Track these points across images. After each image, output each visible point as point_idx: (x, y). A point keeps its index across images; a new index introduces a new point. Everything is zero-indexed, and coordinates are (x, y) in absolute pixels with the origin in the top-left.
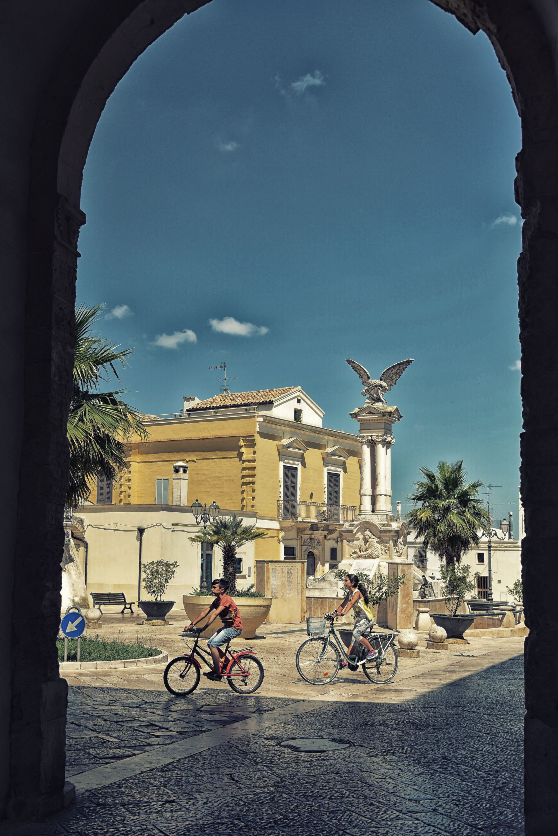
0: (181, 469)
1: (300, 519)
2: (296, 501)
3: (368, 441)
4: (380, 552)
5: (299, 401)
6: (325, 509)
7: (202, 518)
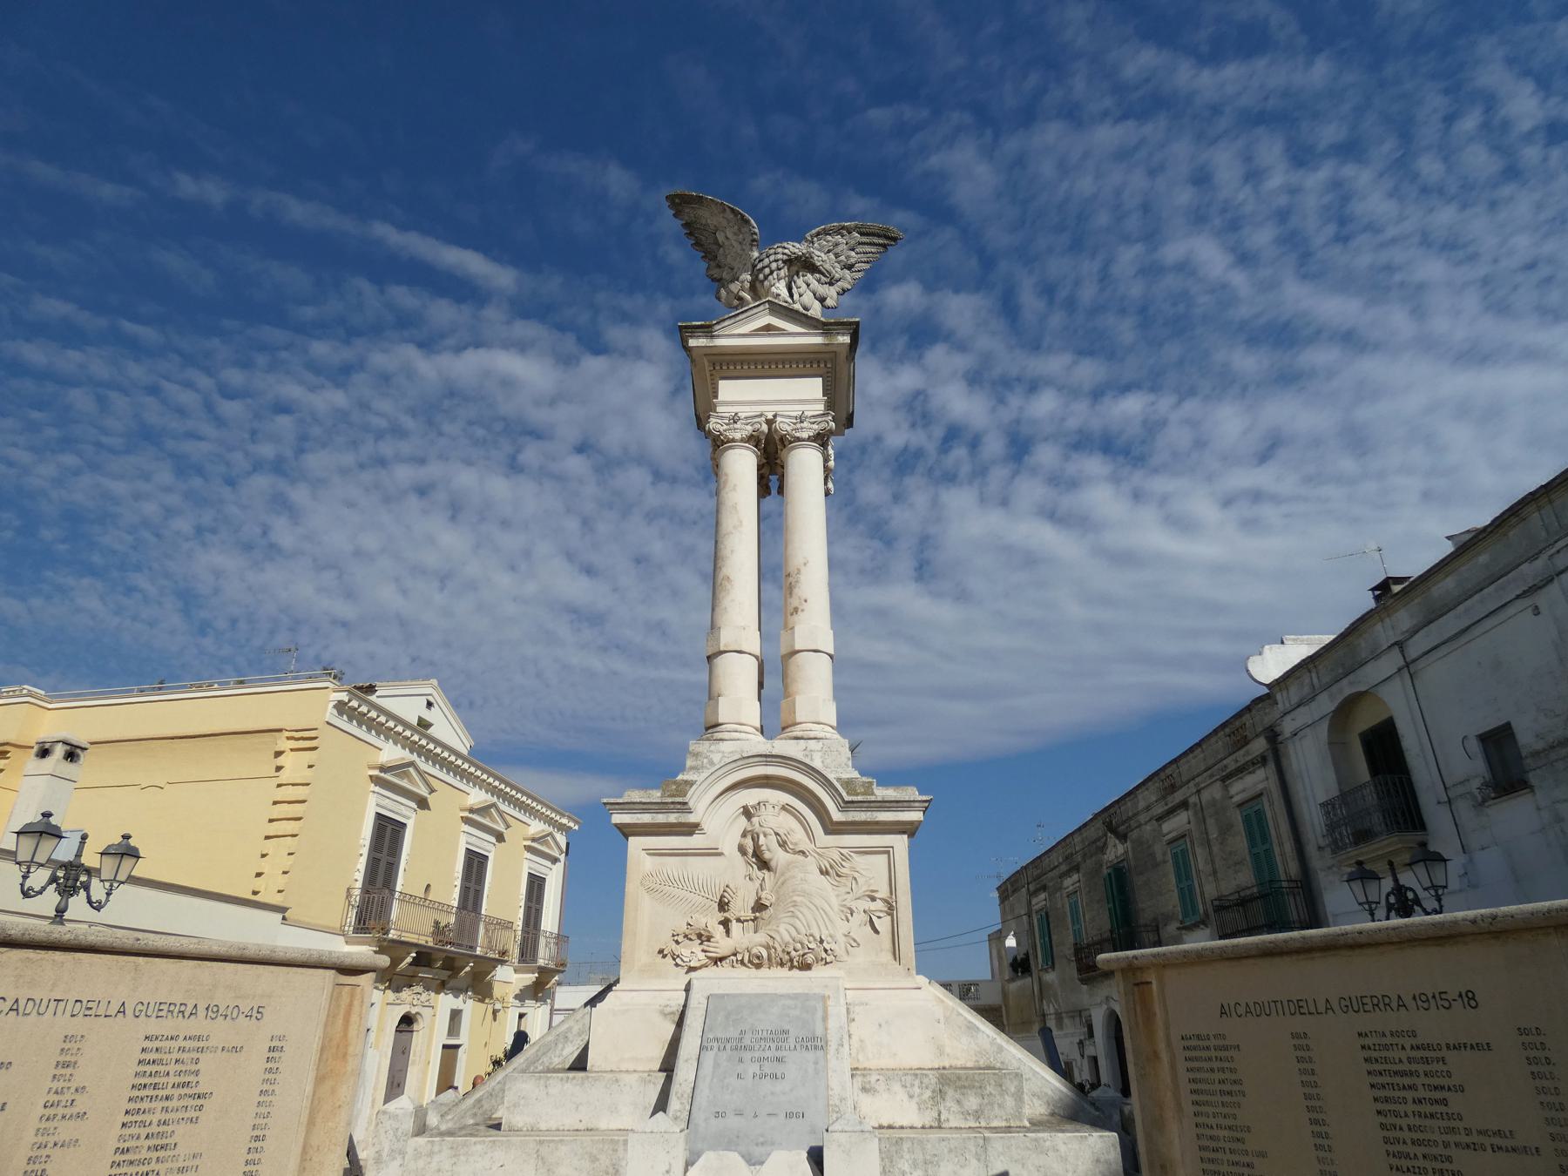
0: (60, 750)
1: (393, 935)
2: (393, 891)
3: (753, 439)
4: (841, 927)
5: (429, 705)
6: (452, 919)
7: (53, 879)
